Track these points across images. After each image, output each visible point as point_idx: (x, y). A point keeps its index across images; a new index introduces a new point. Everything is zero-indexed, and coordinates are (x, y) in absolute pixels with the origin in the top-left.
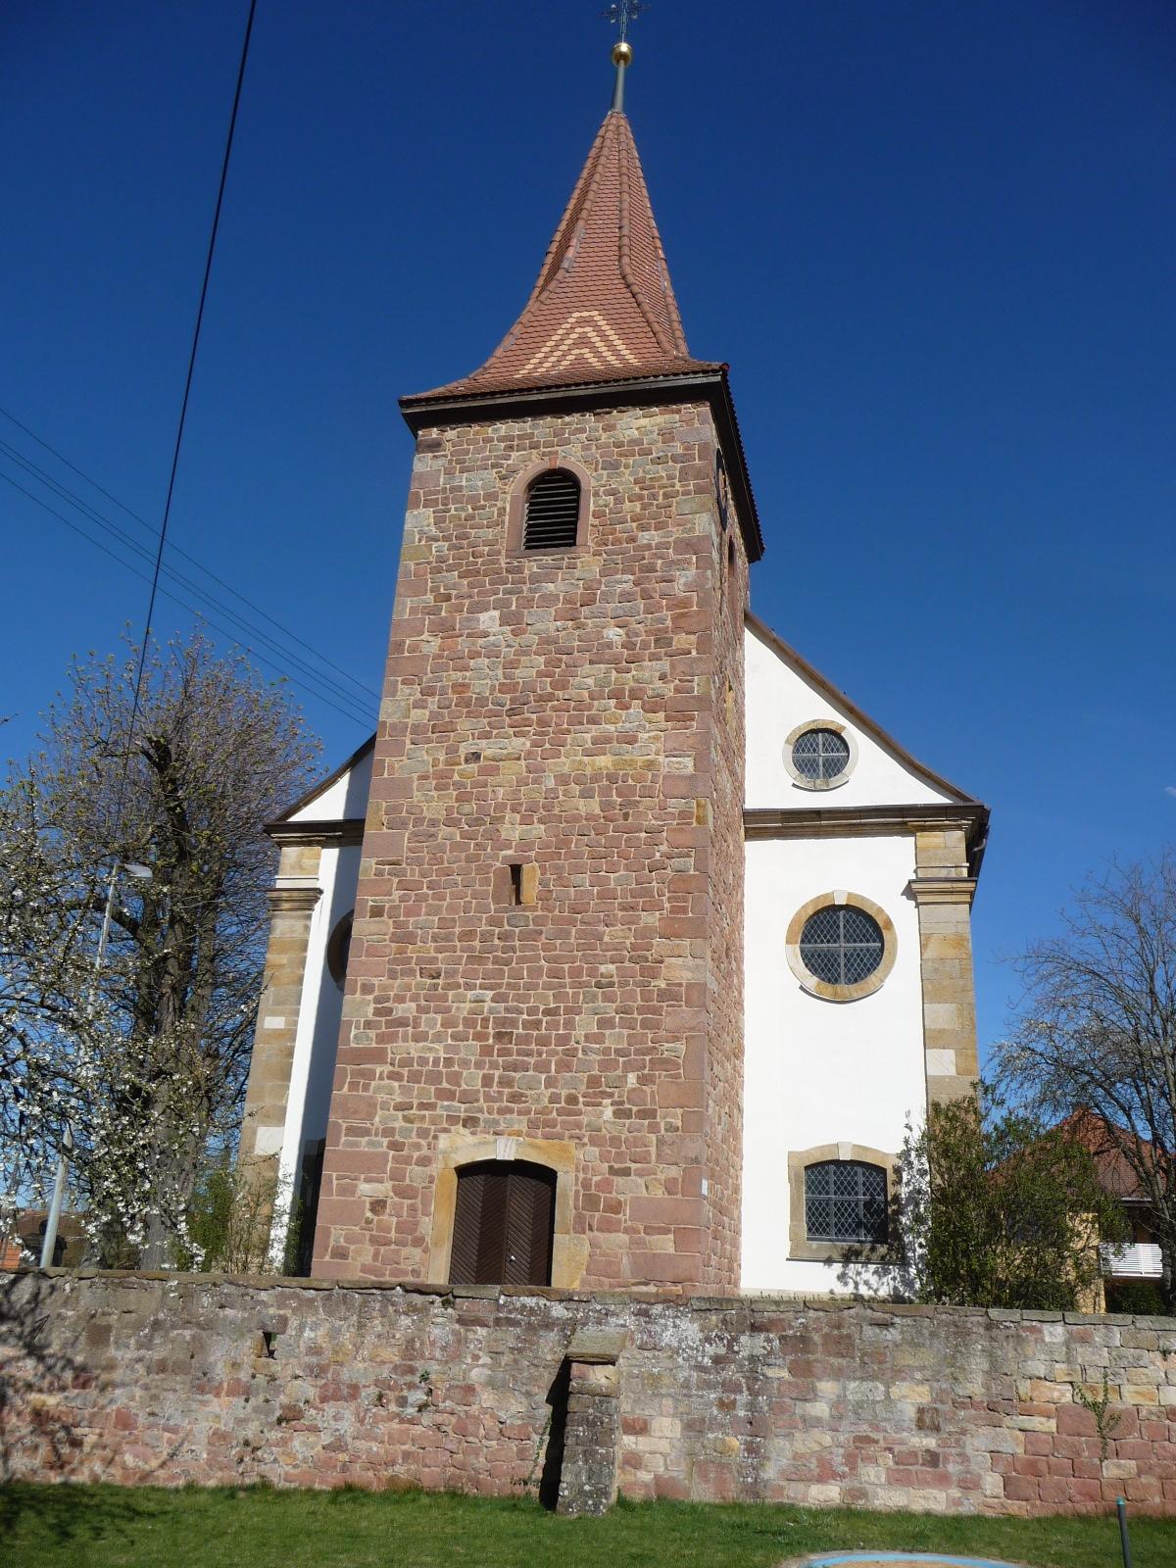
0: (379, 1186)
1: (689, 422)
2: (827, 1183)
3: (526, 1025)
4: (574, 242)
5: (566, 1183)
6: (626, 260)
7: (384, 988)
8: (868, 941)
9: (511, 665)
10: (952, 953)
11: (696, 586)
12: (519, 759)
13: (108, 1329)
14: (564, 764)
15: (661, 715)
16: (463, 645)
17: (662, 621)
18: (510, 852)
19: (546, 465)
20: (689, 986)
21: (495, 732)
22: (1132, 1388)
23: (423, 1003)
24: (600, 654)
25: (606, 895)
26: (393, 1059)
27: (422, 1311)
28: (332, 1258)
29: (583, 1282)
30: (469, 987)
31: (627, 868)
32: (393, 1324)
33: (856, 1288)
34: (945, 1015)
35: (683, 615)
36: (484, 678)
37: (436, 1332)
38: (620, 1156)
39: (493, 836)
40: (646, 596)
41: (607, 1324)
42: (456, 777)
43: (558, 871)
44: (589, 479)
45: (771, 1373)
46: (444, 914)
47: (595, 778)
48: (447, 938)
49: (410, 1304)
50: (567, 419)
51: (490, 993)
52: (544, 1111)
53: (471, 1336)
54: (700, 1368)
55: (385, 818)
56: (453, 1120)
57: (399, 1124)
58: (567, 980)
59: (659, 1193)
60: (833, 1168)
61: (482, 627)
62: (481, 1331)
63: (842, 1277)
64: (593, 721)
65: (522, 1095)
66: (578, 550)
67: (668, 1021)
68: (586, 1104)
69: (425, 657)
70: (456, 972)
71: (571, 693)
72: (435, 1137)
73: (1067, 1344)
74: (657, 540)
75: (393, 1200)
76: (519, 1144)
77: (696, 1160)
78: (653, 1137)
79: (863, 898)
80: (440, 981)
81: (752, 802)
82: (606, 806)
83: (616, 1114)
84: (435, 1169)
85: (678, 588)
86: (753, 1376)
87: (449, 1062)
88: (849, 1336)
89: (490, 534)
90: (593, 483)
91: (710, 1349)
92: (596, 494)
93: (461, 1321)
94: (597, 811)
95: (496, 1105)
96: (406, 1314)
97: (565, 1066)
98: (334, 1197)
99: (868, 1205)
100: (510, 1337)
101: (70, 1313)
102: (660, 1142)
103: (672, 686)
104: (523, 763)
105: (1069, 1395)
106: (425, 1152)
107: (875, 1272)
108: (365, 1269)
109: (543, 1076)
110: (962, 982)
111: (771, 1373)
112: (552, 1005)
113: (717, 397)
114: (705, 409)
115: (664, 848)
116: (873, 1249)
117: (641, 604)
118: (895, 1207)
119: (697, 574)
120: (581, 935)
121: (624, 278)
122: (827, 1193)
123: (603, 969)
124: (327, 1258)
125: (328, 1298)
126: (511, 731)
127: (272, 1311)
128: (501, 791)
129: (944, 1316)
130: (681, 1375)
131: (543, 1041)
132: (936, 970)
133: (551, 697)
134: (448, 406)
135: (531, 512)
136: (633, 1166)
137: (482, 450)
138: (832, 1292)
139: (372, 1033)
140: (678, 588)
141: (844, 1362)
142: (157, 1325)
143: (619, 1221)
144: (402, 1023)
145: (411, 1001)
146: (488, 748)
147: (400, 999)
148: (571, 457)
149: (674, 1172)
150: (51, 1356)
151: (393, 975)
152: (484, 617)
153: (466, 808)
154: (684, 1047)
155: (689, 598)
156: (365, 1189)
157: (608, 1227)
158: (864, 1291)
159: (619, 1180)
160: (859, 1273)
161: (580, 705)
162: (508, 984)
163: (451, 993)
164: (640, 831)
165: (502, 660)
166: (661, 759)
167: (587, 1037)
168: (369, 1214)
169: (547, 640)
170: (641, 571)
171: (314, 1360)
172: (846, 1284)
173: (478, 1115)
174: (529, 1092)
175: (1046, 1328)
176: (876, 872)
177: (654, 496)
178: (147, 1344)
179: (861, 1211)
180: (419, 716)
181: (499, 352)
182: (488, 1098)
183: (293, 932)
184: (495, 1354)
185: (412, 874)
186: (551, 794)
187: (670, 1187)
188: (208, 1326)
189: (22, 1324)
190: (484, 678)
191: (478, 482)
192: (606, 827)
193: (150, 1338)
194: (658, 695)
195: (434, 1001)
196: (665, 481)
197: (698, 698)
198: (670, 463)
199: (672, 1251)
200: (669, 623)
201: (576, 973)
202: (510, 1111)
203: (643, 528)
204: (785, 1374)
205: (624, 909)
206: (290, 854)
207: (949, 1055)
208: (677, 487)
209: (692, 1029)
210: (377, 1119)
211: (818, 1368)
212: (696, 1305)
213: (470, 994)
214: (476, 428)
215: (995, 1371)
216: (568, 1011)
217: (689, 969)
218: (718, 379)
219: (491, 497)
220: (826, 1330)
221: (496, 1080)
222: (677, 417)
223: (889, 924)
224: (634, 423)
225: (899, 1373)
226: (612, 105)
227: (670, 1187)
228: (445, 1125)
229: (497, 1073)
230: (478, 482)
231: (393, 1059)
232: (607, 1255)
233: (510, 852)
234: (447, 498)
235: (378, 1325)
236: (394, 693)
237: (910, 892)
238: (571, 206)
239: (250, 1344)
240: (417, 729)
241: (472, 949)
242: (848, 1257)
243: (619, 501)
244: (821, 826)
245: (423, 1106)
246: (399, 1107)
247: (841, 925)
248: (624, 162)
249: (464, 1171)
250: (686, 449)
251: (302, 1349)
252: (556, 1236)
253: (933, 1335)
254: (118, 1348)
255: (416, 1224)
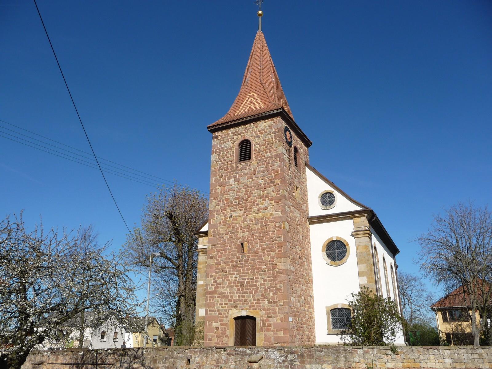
0: (217, 323)
1: (276, 122)
2: (336, 314)
3: (247, 282)
4: (248, 73)
5: (258, 320)
6: (261, 76)
7: (215, 276)
8: (343, 249)
9: (238, 192)
10: (364, 250)
11: (279, 166)
12: (241, 216)
13: (157, 360)
14: (251, 216)
15: (273, 201)
16: (226, 188)
17: (272, 177)
18: (240, 240)
19: (243, 139)
20: (283, 270)
21: (235, 210)
22: (379, 364)
23: (224, 279)
24: (258, 187)
25: (263, 249)
26: (218, 293)
27: (220, 353)
28: (208, 341)
29: (263, 344)
30: (234, 274)
31: (267, 241)
32: (214, 356)
33: (345, 341)
34: (363, 267)
35: (277, 175)
36: (232, 196)
37: (223, 357)
38: (270, 313)
39: (236, 236)
40: (268, 171)
41: (259, 354)
42: (227, 222)
43: (252, 243)
44: (253, 141)
45: (295, 363)
46: (227, 257)
47: (259, 219)
48: (228, 263)
49: (217, 351)
50: (247, 126)
51: (238, 275)
52: (252, 303)
53: (230, 358)
54: (280, 363)
55: (212, 234)
56: (232, 307)
57: (221, 308)
58: (255, 271)
59: (279, 321)
60: (337, 310)
61: (230, 183)
62: (232, 357)
63: (341, 338)
64: (257, 205)
65: (247, 300)
66: (251, 160)
67: (279, 279)
68: (261, 301)
69: (218, 193)
70: (230, 270)
71: (252, 198)
72: (229, 311)
73: (363, 354)
74: (270, 155)
75: (220, 327)
76: (247, 311)
77: (287, 313)
78: (277, 308)
79: (340, 238)
80: (227, 273)
81: (311, 215)
82: (262, 226)
83: (268, 303)
84: (229, 319)
85: (275, 168)
86: (291, 364)
87: (230, 293)
88: (313, 354)
89: (231, 159)
90: (254, 142)
91: (282, 358)
92: (255, 145)
93: (228, 354)
94: (260, 228)
95: (241, 303)
96: (216, 353)
97: (256, 292)
98: (208, 327)
99: (347, 319)
100: (238, 358)
101: (149, 357)
102: (279, 309)
103: (275, 194)
104: (242, 217)
105: (364, 366)
106: (227, 315)
107: (349, 337)
108: (216, 343)
109: (251, 295)
110: (367, 258)
111: (295, 363)
112: (252, 277)
113: (283, 114)
114: (280, 118)
115: (276, 235)
116: (348, 331)
117: (267, 173)
118: (353, 319)
119: (280, 163)
120: (258, 259)
121: (261, 82)
122: (336, 317)
123: (263, 267)
124: (207, 341)
125: (200, 351)
126: (239, 209)
127: (189, 354)
128: (237, 225)
129: (334, 348)
130: (276, 365)
131: (251, 286)
132: (360, 255)
133: (247, 200)
134: (218, 127)
135: (240, 151)
136: (273, 315)
137: (228, 136)
138: (339, 342)
139: (213, 287)
140: (275, 168)
141: (312, 360)
142: (166, 358)
143: (270, 329)
144: (219, 284)
145: (221, 278)
146: (234, 214)
147: (218, 278)
148: (248, 136)
149: (282, 316)
150: (147, 366)
151: (216, 273)
152: (231, 180)
153: (230, 230)
154: (283, 285)
155: (278, 170)
156: (214, 324)
157: (268, 330)
158: (347, 342)
159: (270, 319)
160: (345, 337)
161: (254, 201)
162: (242, 273)
163: (230, 276)
164: (270, 232)
165: (235, 191)
166: (274, 213)
167: (260, 284)
168: (215, 330)
169: (246, 185)
170: (267, 164)
171: (198, 365)
172: (342, 340)
173: (238, 305)
174: (248, 299)
175: (358, 350)
176: (343, 230)
177: (268, 144)
178: (164, 363)
179: (345, 321)
180: (218, 207)
181: (231, 108)
182: (240, 301)
183: (203, 259)
184: (235, 362)
185: (219, 247)
186: (249, 224)
187: (282, 320)
188: (176, 358)
189: (140, 359)
190: (232, 196)
191: (226, 145)
192: (262, 231)
193: (165, 361)
194: (272, 196)
195: (226, 278)
196: (271, 139)
197: (281, 196)
198: (272, 134)
199: (283, 335)
200: (274, 177)
201: (257, 269)
202: (245, 304)
203: (266, 153)
204: (299, 364)
205: (267, 252)
206: (201, 239)
207: (365, 278)
208: (274, 141)
209: (284, 280)
210: (216, 308)
211: (306, 362)
212: (278, 348)
213: (234, 276)
214: (226, 131)
215: (346, 361)
216: (256, 278)
217: (283, 266)
218: (281, 110)
219: (230, 149)
220: (307, 353)
221: (241, 296)
222: (273, 121)
223: (348, 244)
224: (263, 125)
225: (324, 362)
226: (258, 30)
227: (282, 320)
228: (230, 308)
229: (241, 295)
230: (226, 145)
231: (218, 293)
232: (268, 337)
233: (240, 240)
234: (220, 151)
235: (210, 356)
236: (212, 202)
237: (352, 235)
238: (249, 61)
239: (185, 361)
240: (218, 211)
241: (233, 265)
242: (342, 333)
243: (260, 146)
244: (328, 219)
245: (226, 304)
246: (220, 304)
247: (336, 245)
248: (261, 47)
249: (236, 319)
250: (275, 130)
251: (195, 362)
252: (258, 334)
253: (332, 353)
254: (159, 364)
255: (226, 332)
